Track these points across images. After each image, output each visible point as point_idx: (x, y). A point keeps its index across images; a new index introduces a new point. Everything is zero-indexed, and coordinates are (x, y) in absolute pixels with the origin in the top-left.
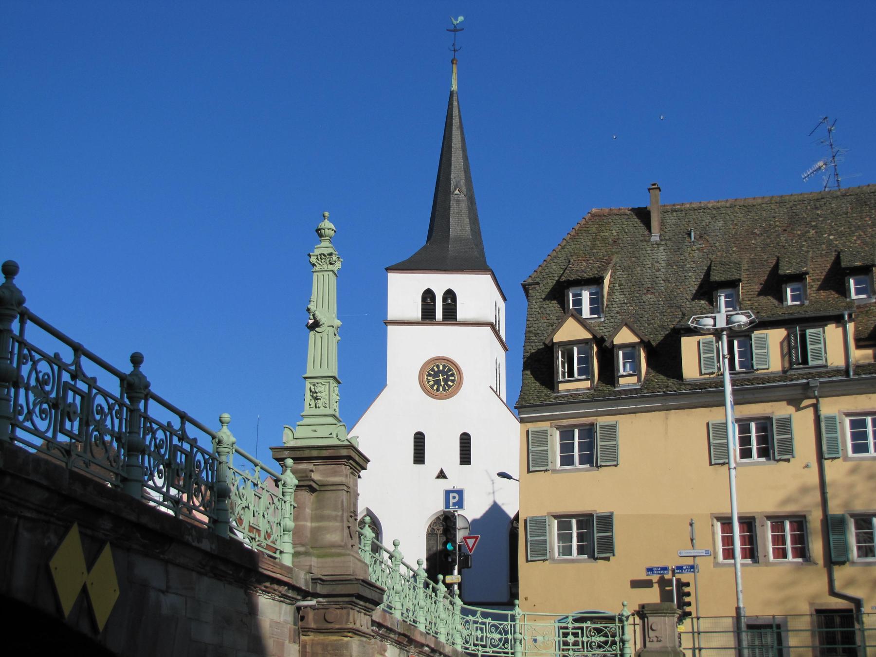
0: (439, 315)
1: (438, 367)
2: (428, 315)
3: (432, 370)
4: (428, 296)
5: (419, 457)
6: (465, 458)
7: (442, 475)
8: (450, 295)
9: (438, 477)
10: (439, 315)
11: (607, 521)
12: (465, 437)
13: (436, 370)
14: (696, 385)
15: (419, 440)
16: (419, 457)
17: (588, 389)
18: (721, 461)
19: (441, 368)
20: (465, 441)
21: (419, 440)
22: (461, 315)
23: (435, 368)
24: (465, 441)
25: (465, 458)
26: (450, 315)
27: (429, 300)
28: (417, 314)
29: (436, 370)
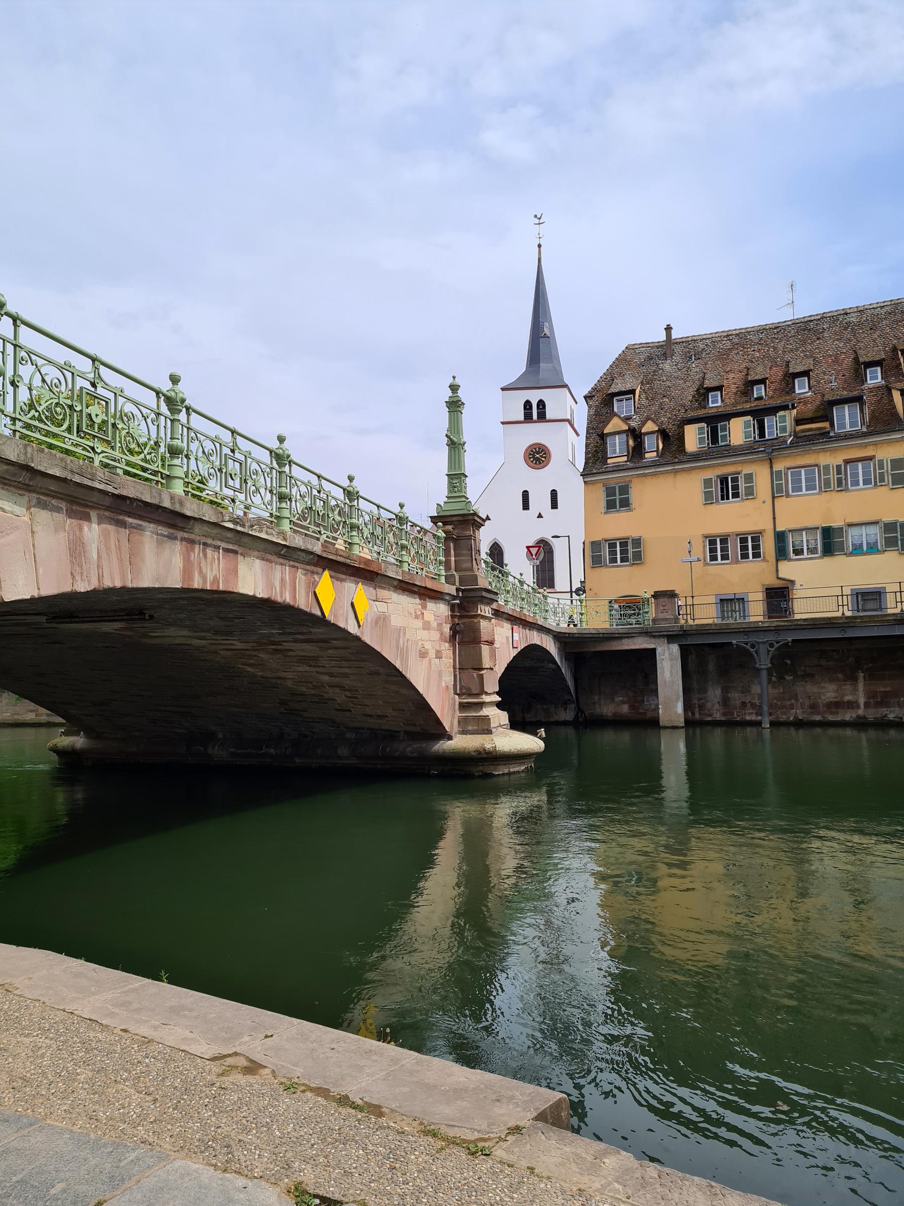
0: (535, 416)
1: (535, 449)
2: (528, 417)
3: (532, 451)
4: (528, 405)
5: (526, 506)
6: (554, 505)
7: (540, 516)
8: (541, 404)
9: (538, 517)
10: (535, 416)
11: (637, 542)
12: (553, 492)
14: (693, 455)
15: (525, 495)
16: (526, 506)
17: (626, 461)
18: (709, 502)
20: (554, 494)
21: (525, 495)
22: (549, 416)
24: (554, 494)
25: (554, 505)
26: (542, 417)
27: (528, 407)
28: (522, 418)
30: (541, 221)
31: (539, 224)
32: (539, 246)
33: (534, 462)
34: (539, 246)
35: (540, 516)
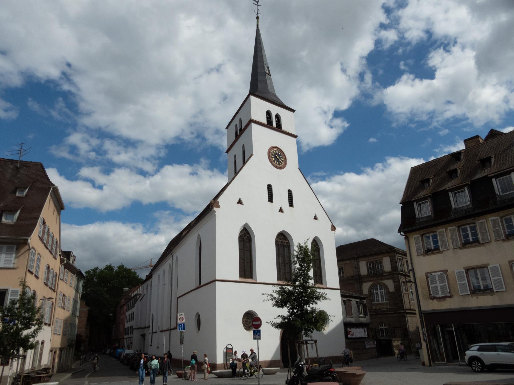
0: (274, 124)
5: (271, 200)
6: (291, 204)
8: (278, 117)
10: (274, 124)
13: (275, 153)
15: (270, 188)
16: (271, 200)
19: (277, 153)
20: (290, 193)
21: (270, 188)
23: (274, 151)
24: (290, 193)
25: (291, 204)
26: (279, 128)
28: (265, 121)
29: (275, 153)
30: (259, 4)
31: (258, 5)
32: (258, 18)
33: (275, 162)
34: (258, 18)
35: (281, 210)
